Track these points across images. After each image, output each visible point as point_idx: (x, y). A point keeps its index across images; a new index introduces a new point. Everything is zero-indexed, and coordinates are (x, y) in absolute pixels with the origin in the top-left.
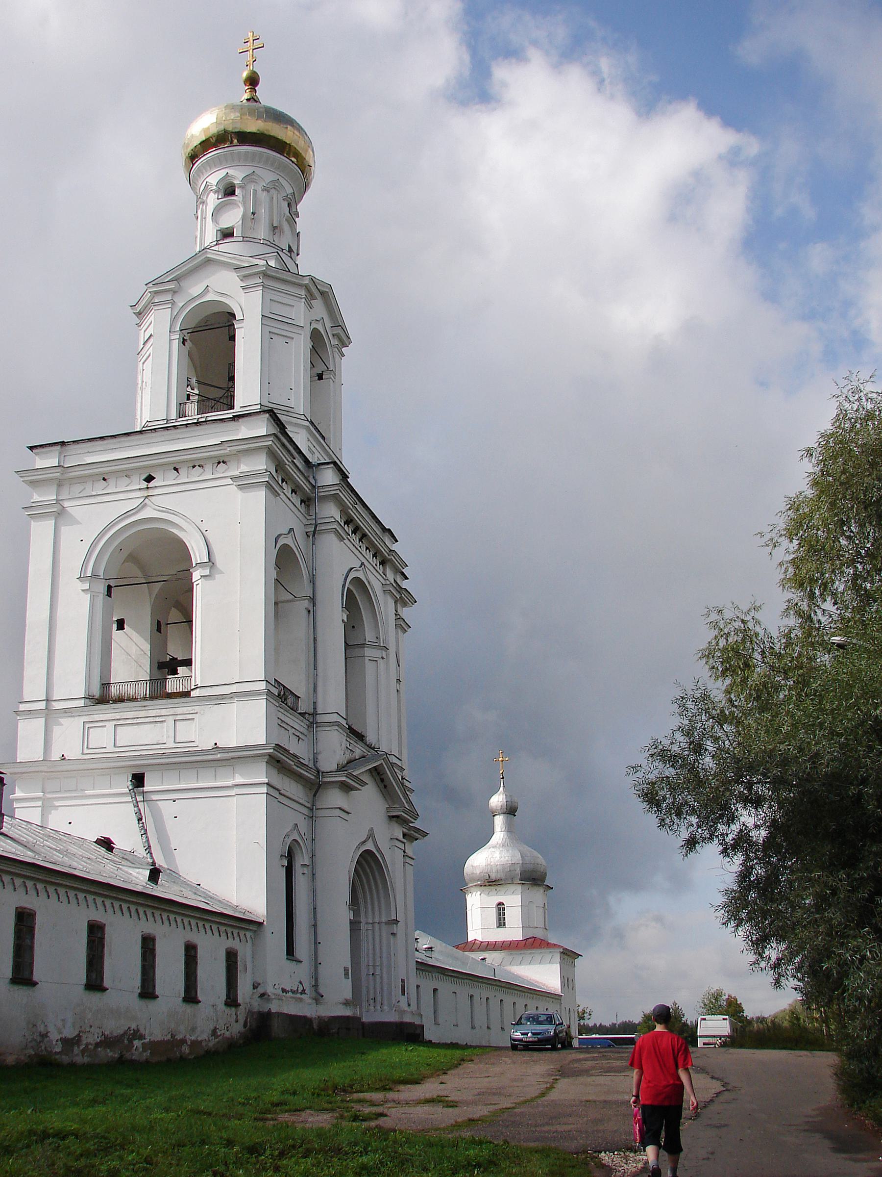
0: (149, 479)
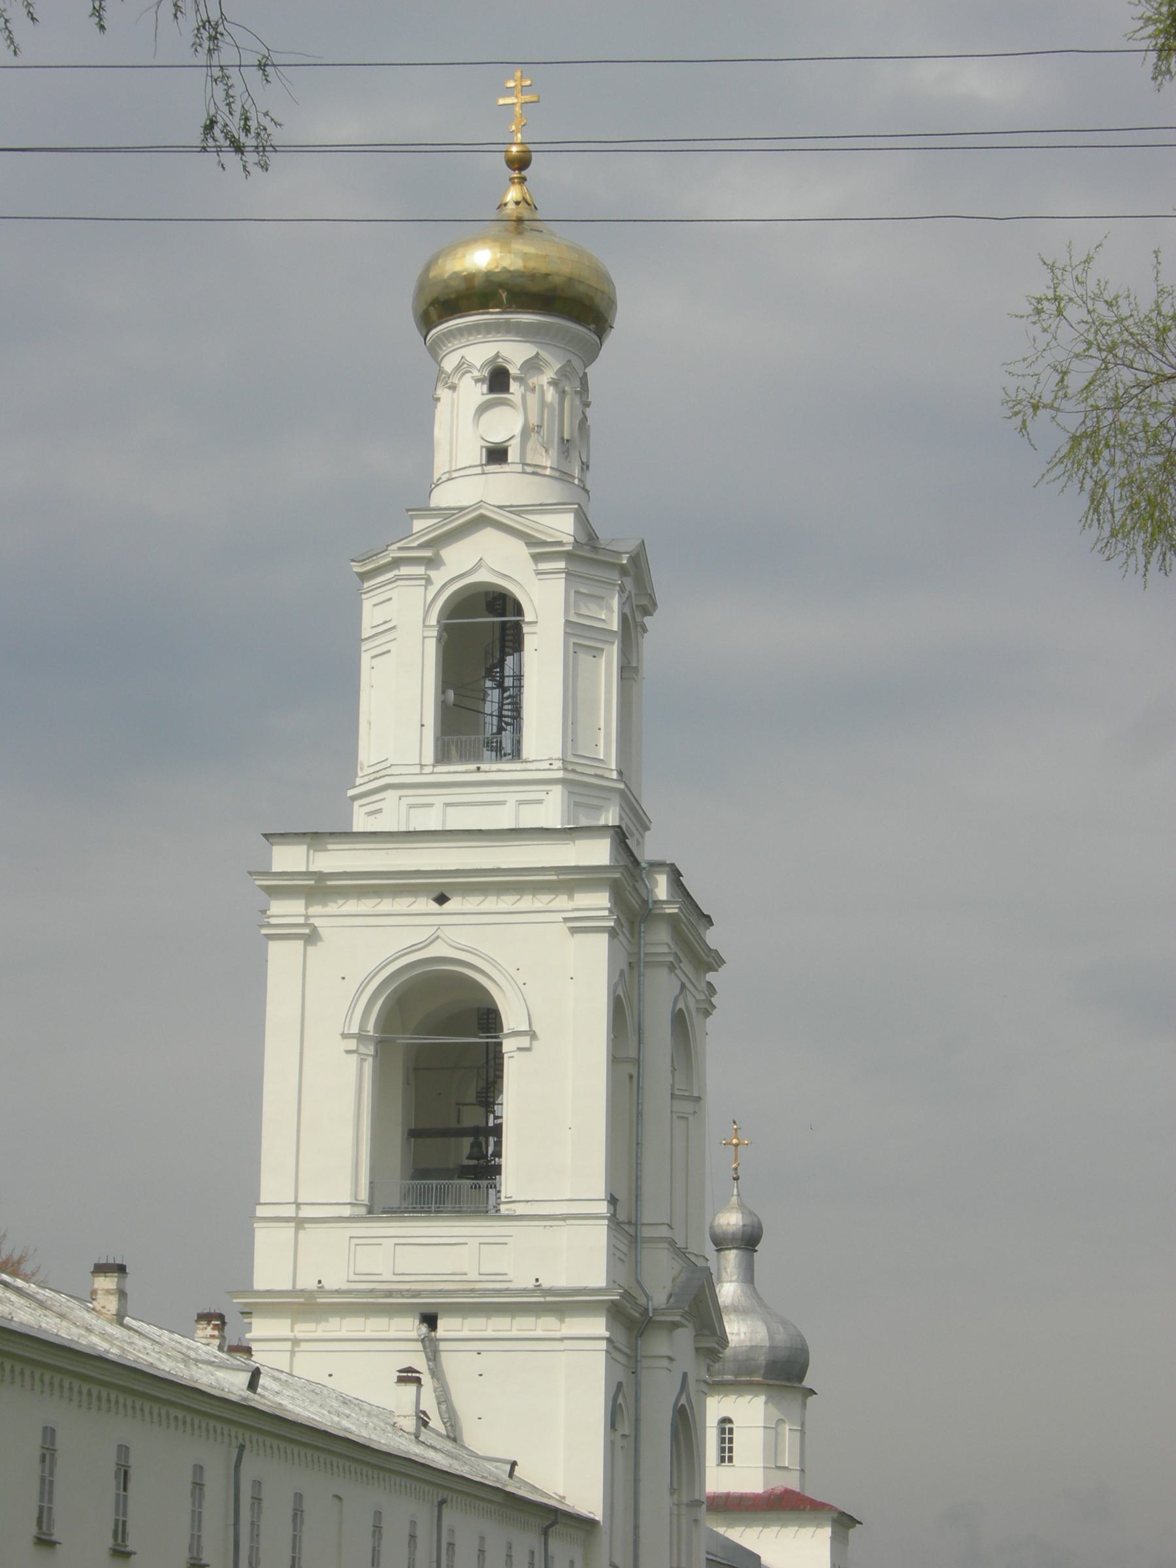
0: (441, 899)
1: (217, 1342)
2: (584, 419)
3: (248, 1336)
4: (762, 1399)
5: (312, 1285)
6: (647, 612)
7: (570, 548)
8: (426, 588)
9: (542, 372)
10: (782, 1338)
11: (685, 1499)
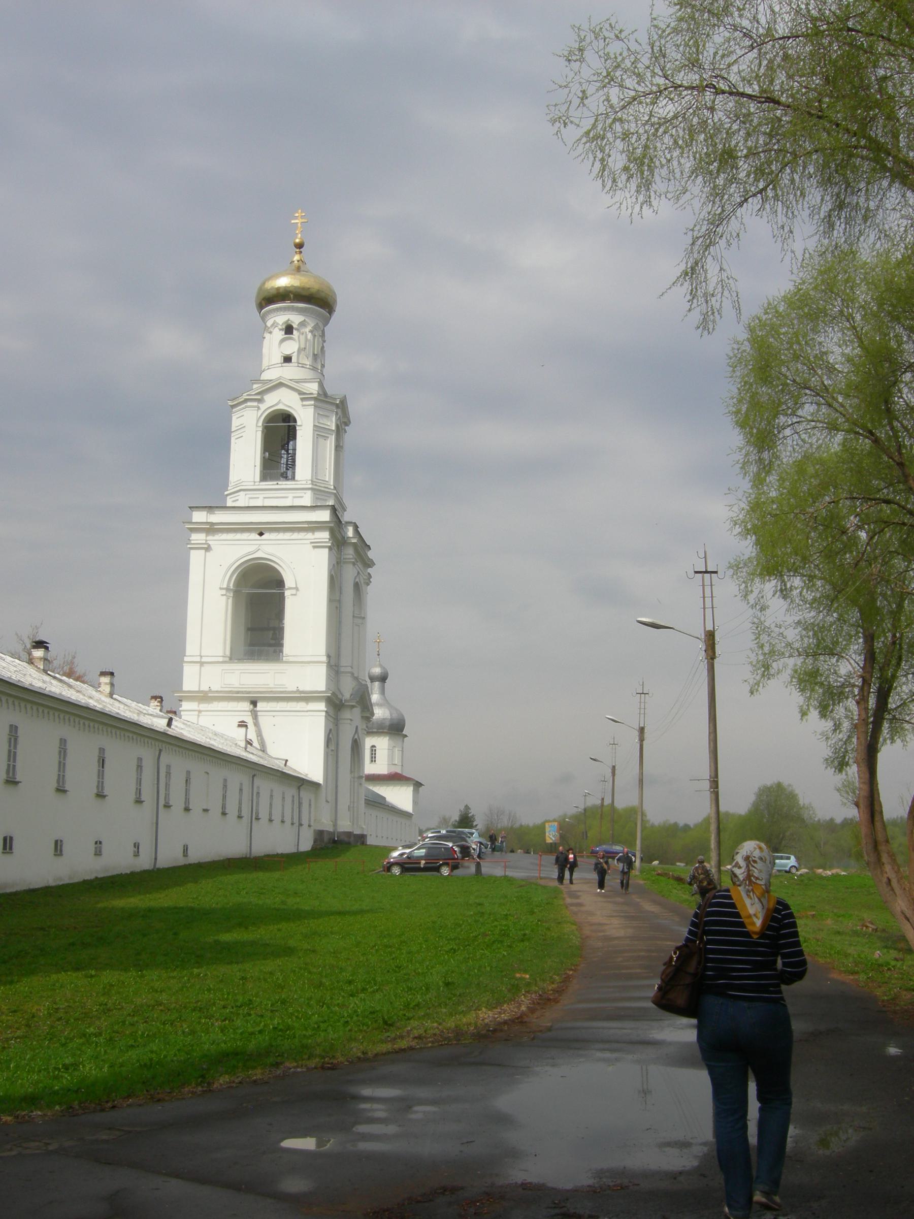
0: (261, 534)
1: (159, 708)
2: (323, 347)
4: (388, 738)
5: (207, 689)
10: (395, 715)
11: (356, 775)
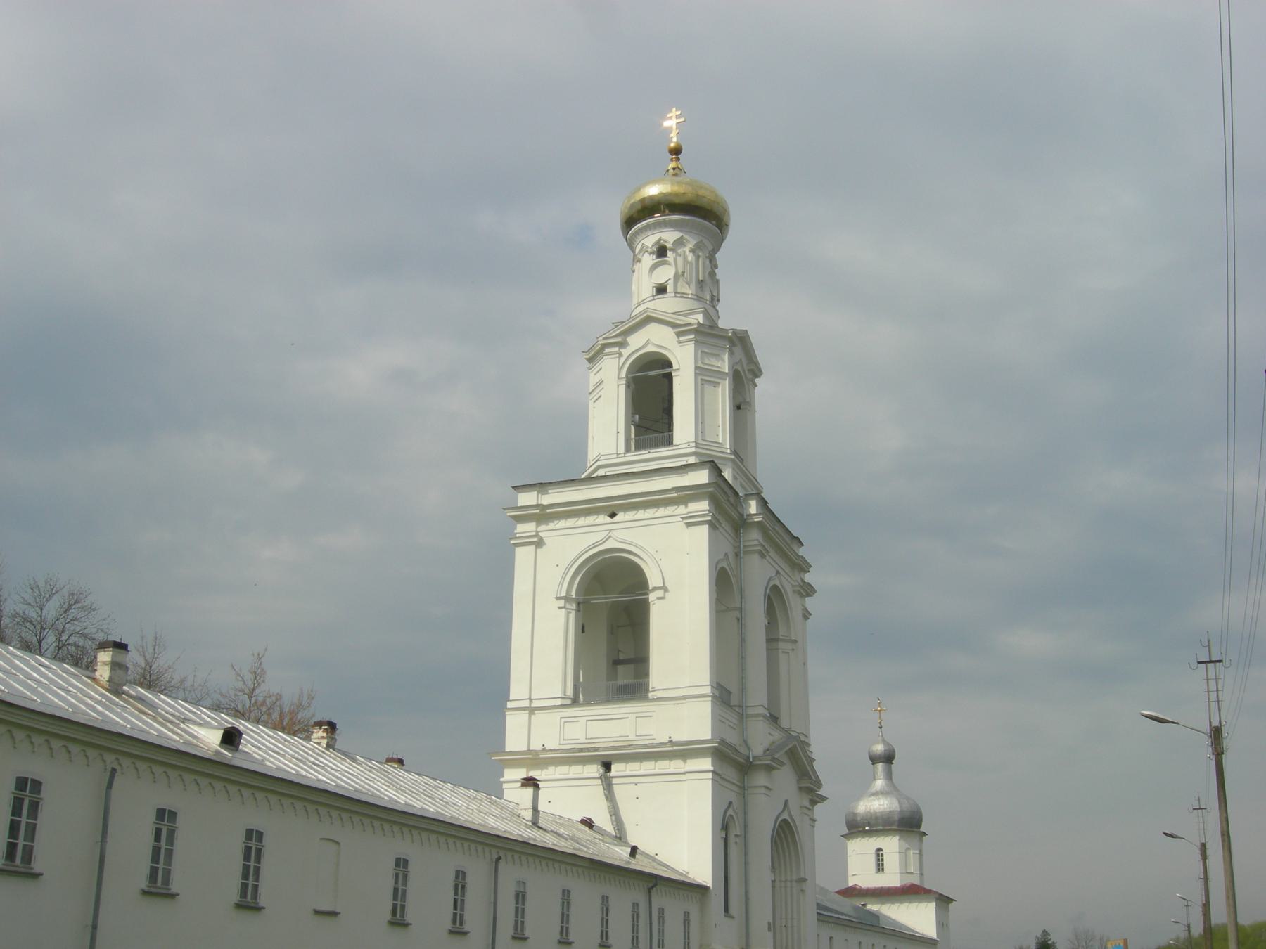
0: (613, 515)
3: (501, 780)
4: (898, 837)
5: (539, 748)
6: (758, 376)
7: (695, 326)
8: (619, 359)
9: (685, 246)
10: (906, 806)
11: (795, 878)
